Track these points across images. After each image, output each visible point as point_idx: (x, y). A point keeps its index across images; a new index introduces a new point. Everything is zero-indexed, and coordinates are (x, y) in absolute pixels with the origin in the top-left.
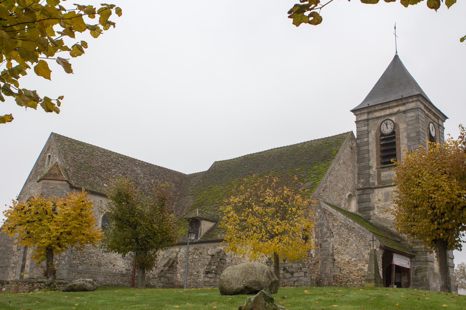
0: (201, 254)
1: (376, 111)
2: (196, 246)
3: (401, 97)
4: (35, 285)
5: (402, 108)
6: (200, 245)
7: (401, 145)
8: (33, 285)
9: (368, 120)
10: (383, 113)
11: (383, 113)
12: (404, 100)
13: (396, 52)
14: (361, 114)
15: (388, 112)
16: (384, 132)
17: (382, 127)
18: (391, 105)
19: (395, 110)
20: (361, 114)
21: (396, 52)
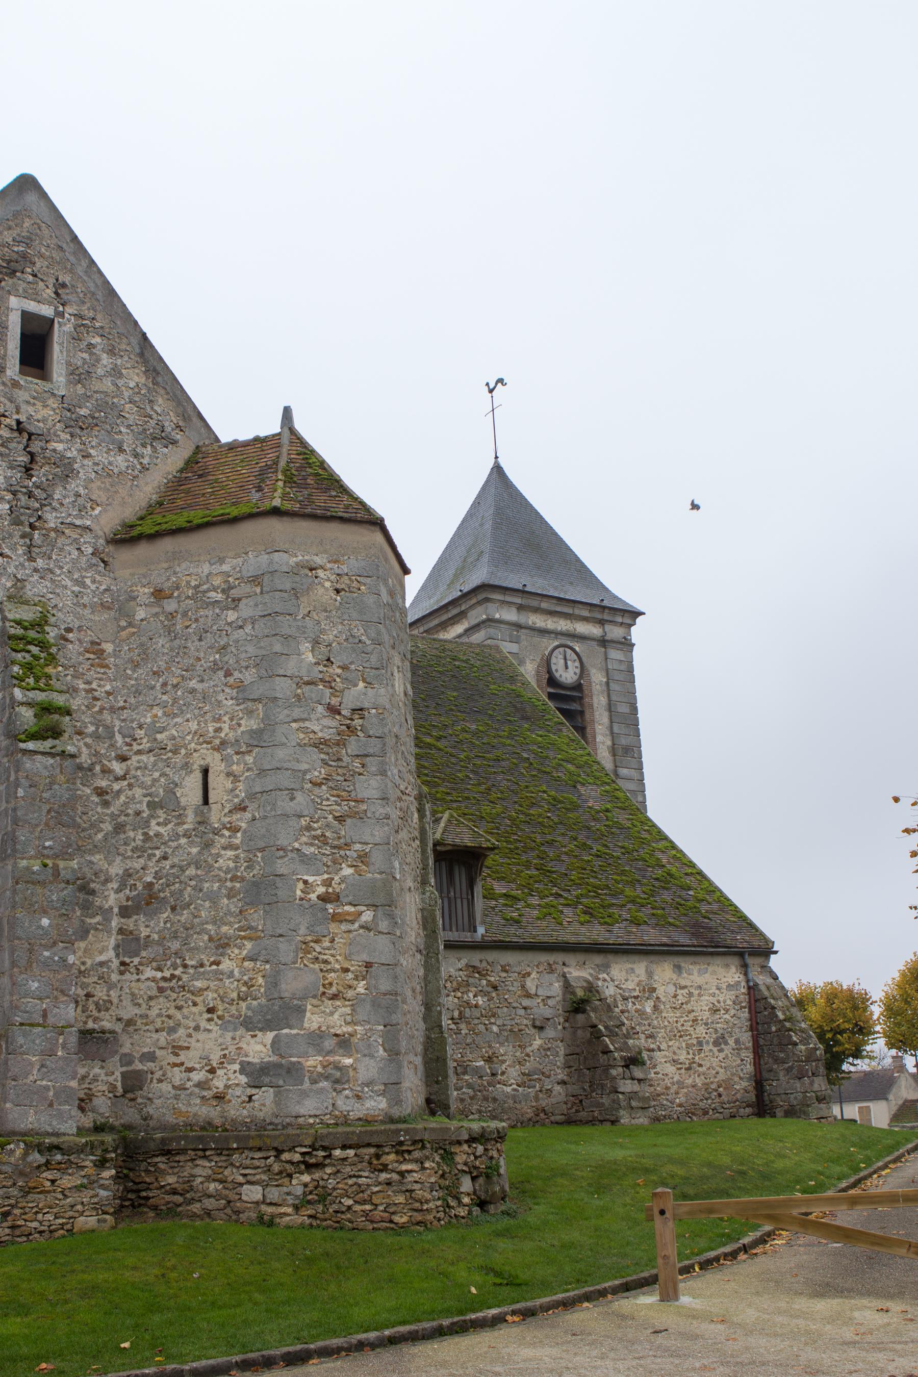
0: (495, 988)
1: (536, 610)
2: (475, 958)
3: (520, 587)
4: (462, 1156)
5: (594, 630)
6: (491, 956)
7: (596, 725)
8: (448, 1157)
9: (518, 626)
10: (550, 623)
11: (550, 623)
12: (607, 611)
13: (496, 457)
14: (503, 602)
15: (563, 625)
16: (557, 675)
17: (553, 660)
18: (577, 612)
19: (582, 628)
20: (503, 602)
21: (496, 457)
